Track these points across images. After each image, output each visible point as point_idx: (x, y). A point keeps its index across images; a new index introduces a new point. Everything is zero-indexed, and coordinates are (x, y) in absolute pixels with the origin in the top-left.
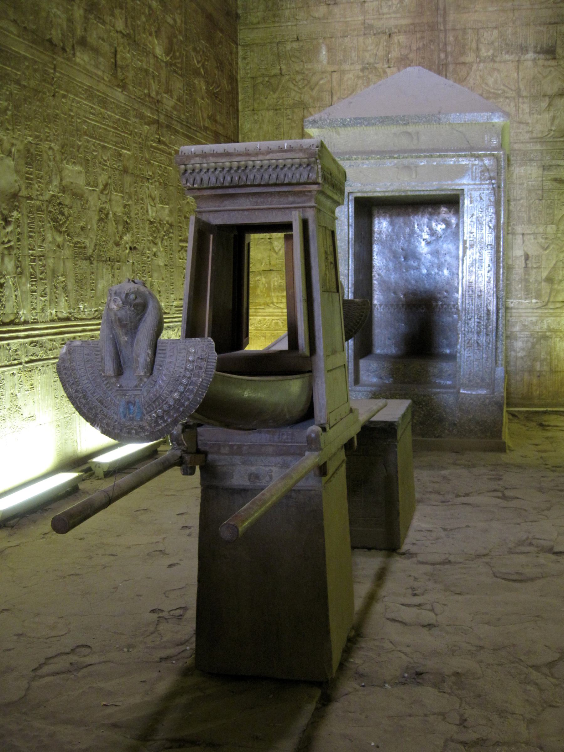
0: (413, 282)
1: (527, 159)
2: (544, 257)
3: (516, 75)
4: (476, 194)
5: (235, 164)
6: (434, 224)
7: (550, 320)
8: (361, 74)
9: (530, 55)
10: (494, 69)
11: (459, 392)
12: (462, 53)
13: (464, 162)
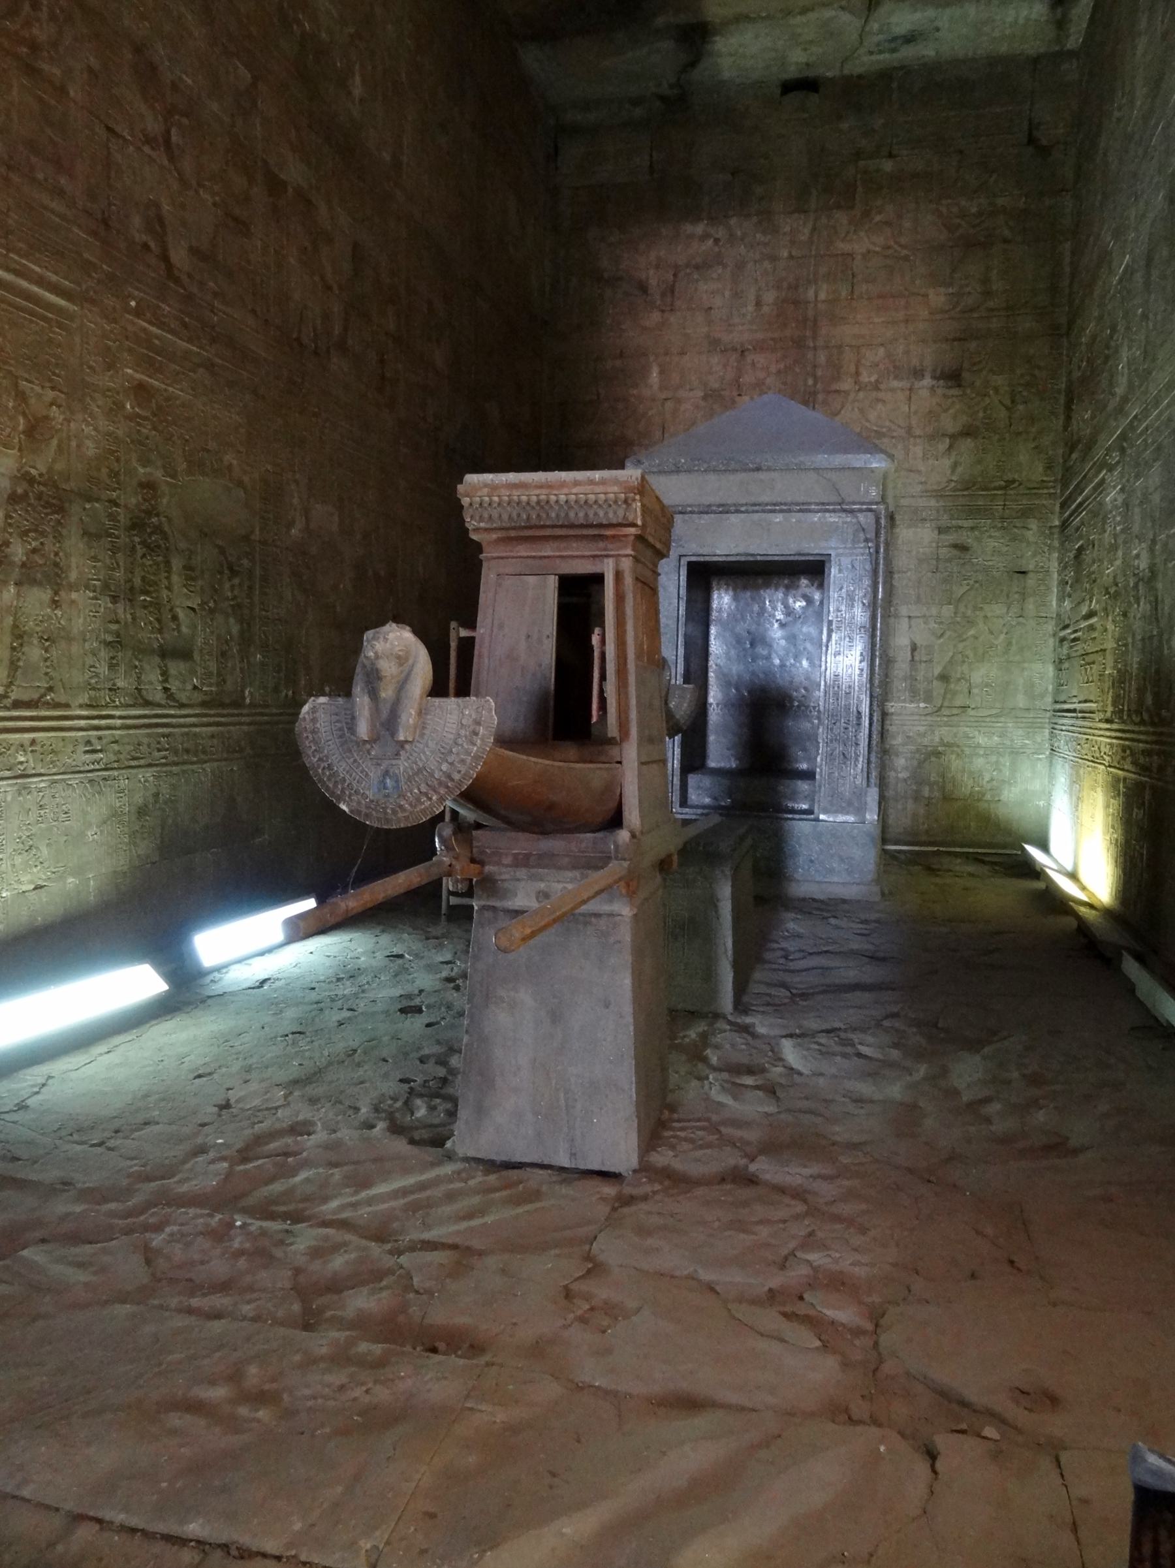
0: (761, 676)
1: (918, 518)
2: (936, 647)
4: (846, 561)
6: (791, 601)
7: (944, 730)
8: (702, 404)
9: (927, 381)
10: (878, 400)
11: (817, 820)
12: (837, 378)
13: (832, 518)
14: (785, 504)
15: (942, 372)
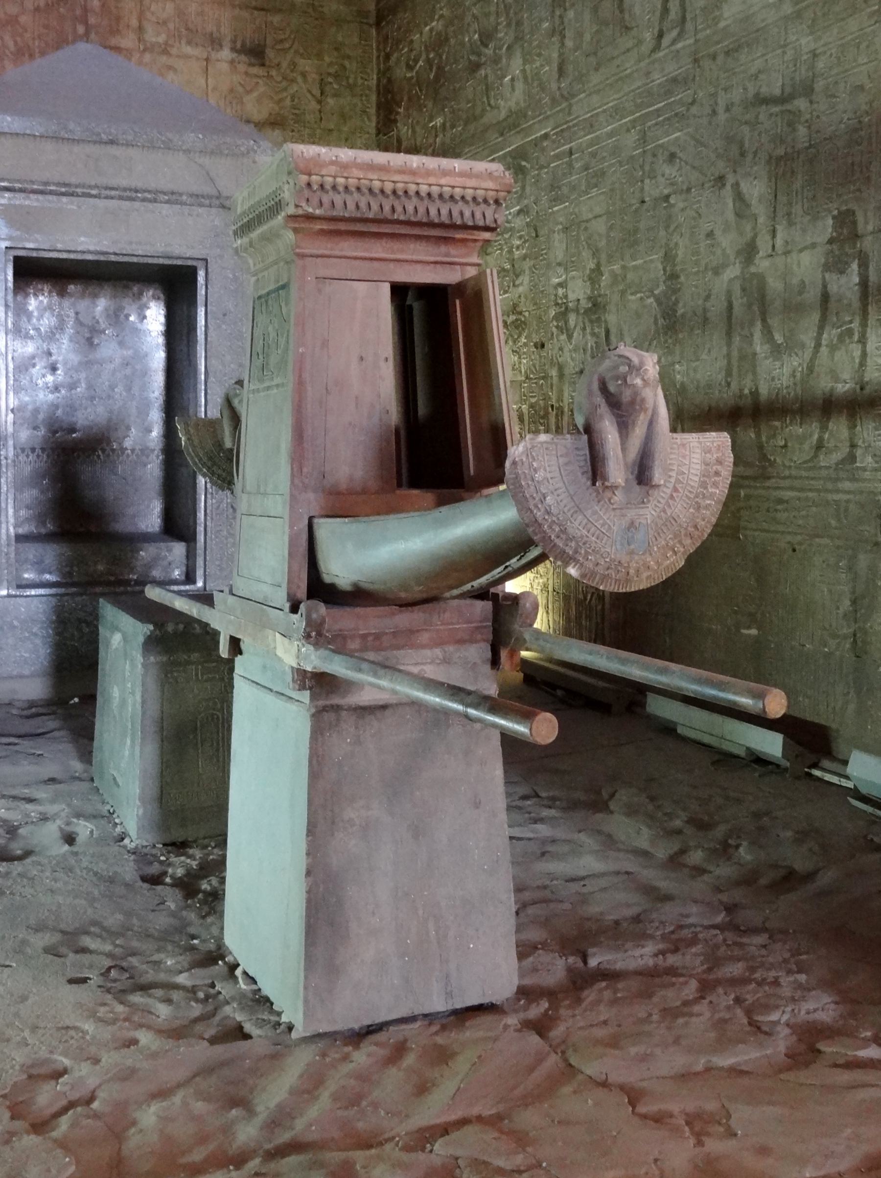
3: (203, 81)
5: (388, 187)
9: (226, 54)
10: (170, 68)
14: (149, 192)
15: (243, 45)
